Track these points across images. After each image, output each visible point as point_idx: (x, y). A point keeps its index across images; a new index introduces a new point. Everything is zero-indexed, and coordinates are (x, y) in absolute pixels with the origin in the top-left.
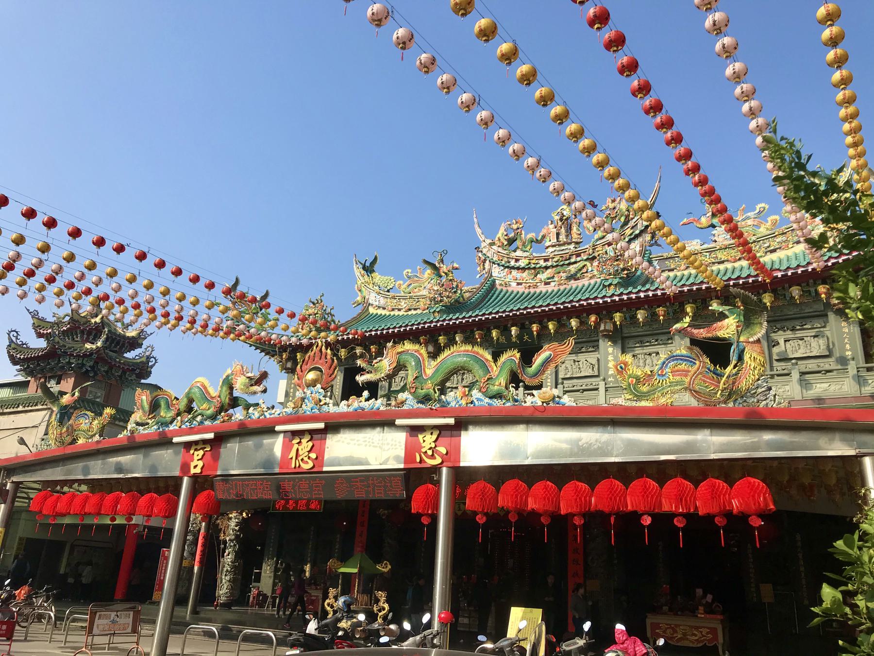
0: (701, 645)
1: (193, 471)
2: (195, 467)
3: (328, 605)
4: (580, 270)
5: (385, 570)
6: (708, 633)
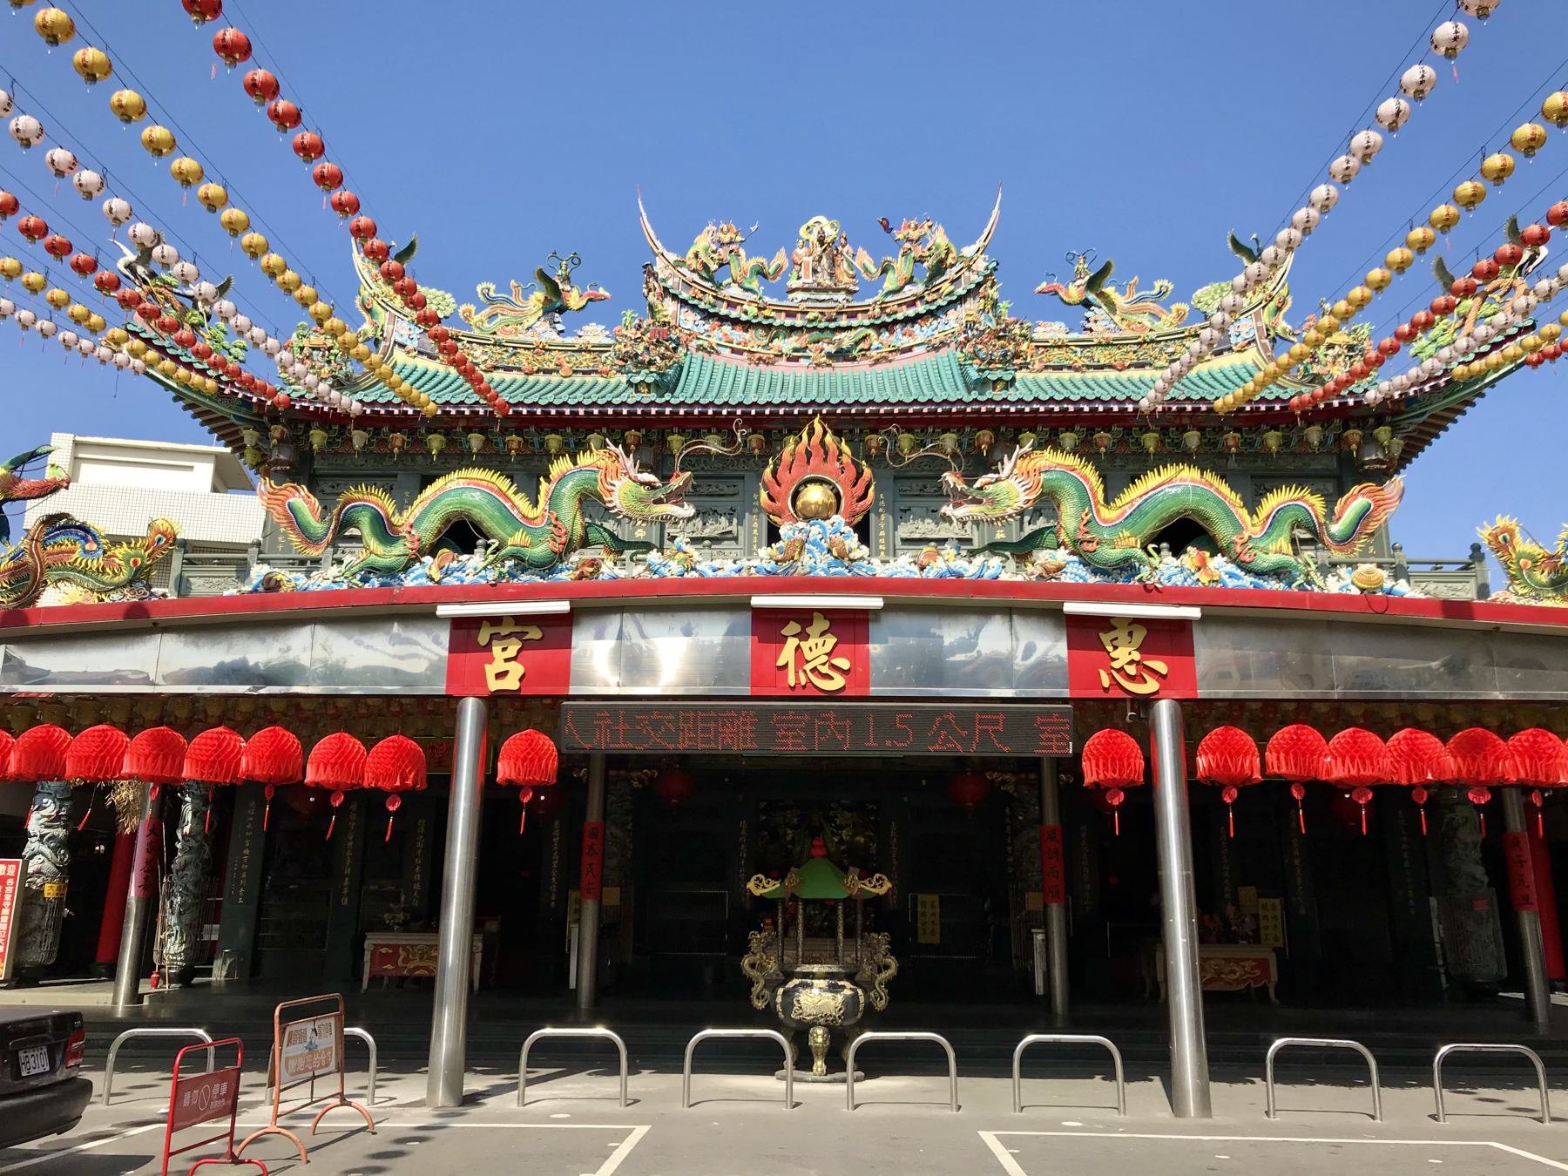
0: (1243, 986)
1: (494, 685)
2: (501, 675)
3: (753, 966)
4: (857, 343)
5: (882, 891)
6: (1253, 968)
